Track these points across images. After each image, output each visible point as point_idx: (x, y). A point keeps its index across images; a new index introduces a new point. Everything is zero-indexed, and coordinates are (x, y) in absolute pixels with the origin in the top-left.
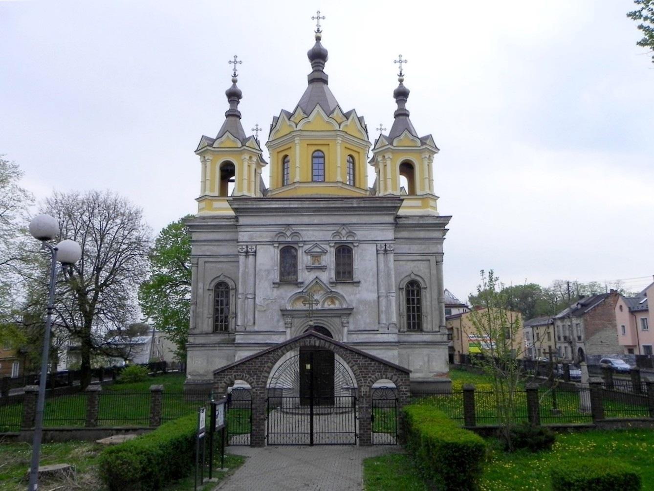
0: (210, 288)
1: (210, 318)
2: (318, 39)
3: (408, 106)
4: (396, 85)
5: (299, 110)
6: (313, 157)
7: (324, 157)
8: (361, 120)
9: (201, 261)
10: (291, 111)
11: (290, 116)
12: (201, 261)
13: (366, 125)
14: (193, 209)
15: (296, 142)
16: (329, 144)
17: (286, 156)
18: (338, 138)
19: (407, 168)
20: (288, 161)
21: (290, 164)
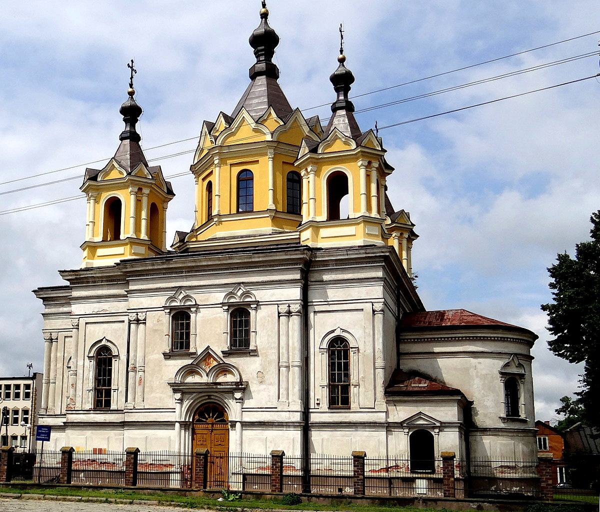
0: (91, 355)
9: (82, 321)
10: (215, 122)
14: (80, 261)
15: (216, 162)
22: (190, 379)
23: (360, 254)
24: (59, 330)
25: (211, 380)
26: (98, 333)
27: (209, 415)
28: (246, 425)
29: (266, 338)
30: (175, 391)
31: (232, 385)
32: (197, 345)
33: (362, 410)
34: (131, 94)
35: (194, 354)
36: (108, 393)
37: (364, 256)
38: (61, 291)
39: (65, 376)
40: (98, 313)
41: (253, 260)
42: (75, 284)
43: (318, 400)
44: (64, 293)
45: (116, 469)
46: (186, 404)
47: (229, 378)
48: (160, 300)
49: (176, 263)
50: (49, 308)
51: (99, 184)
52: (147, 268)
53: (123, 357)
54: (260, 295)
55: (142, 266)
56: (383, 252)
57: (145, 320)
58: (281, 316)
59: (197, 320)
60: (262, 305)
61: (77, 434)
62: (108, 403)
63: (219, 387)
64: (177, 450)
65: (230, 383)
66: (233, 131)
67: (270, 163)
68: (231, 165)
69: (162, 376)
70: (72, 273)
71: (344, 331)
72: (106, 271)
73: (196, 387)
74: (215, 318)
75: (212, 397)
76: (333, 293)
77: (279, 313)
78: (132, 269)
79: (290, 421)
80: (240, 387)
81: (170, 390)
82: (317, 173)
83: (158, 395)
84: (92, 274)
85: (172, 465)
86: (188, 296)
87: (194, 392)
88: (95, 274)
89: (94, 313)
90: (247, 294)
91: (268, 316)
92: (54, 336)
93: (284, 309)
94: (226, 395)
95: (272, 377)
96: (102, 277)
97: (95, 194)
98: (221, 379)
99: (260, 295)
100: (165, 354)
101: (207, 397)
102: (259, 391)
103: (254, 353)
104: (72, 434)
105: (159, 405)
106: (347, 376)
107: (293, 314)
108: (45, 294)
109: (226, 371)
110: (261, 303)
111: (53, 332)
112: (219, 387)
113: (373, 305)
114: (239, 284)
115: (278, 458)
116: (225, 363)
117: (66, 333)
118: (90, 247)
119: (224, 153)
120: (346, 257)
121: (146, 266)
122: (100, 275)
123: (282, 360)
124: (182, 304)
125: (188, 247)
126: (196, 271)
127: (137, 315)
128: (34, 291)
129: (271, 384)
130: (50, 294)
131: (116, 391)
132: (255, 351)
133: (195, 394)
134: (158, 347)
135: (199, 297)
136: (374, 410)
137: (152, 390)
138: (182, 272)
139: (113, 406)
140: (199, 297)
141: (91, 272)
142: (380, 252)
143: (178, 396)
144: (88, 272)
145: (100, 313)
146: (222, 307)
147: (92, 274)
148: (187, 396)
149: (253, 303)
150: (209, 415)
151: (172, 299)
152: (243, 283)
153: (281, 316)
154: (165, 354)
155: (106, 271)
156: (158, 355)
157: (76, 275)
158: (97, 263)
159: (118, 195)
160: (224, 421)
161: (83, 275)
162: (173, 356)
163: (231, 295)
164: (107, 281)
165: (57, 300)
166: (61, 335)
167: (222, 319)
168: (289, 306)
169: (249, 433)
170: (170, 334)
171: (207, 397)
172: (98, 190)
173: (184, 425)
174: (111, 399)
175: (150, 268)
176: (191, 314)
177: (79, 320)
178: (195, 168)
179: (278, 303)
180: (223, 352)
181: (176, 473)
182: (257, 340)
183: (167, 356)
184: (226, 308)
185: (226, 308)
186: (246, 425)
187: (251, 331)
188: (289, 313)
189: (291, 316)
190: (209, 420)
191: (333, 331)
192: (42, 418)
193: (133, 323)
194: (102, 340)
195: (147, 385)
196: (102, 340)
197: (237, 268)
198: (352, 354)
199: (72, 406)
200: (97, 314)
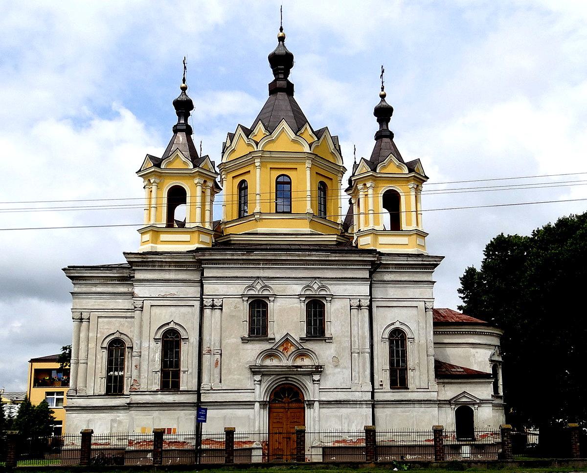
0: (157, 337)
1: (156, 372)
2: (281, 39)
3: (392, 126)
4: (377, 101)
5: (260, 125)
6: (277, 183)
7: (290, 183)
8: (335, 140)
11: (248, 132)
12: (147, 304)
13: (339, 146)
14: (139, 245)
15: (257, 164)
16: (297, 169)
17: (243, 181)
18: (307, 161)
19: (392, 201)
20: (246, 188)
21: (249, 190)
22: (268, 362)
23: (418, 261)
24: (92, 310)
25: (290, 363)
26: (165, 316)
27: (284, 395)
28: (324, 404)
30: (254, 373)
31: (312, 368)
32: (276, 331)
33: (419, 390)
34: (184, 89)
35: (274, 339)
37: (421, 263)
39: (98, 357)
40: (165, 296)
41: (330, 259)
42: (139, 267)
43: (381, 381)
44: (102, 273)
45: (186, 447)
46: (265, 385)
47: (307, 362)
48: (238, 288)
49: (256, 255)
50: (79, 287)
51: (163, 171)
53: (194, 339)
54: (335, 289)
55: (222, 255)
56: (435, 261)
58: (353, 309)
59: (274, 308)
60: (336, 298)
61: (143, 414)
63: (299, 370)
64: (257, 429)
65: (310, 367)
66: (273, 138)
67: (308, 172)
68: (270, 168)
69: (240, 359)
71: (402, 324)
73: (277, 370)
74: (293, 307)
75: (289, 379)
76: (393, 292)
77: (351, 306)
79: (362, 399)
80: (319, 370)
81: (248, 374)
82: (375, 188)
83: (235, 377)
84: (161, 258)
85: (251, 442)
86: (266, 286)
87: (273, 375)
88: (165, 258)
90: (322, 288)
91: (341, 309)
92: (85, 316)
93: (355, 303)
94: (304, 378)
95: (345, 361)
96: (170, 262)
97: (157, 181)
98: (299, 362)
99: (335, 289)
100: (243, 339)
101: (284, 379)
102: (334, 374)
104: (136, 415)
105: (237, 386)
106: (405, 361)
108: (77, 273)
109: (304, 355)
110: (334, 297)
111: (84, 312)
112: (299, 370)
113: (425, 304)
114: (315, 278)
115: (438, 432)
116: (303, 348)
117: (100, 313)
118: (154, 231)
119: (266, 158)
122: (169, 260)
123: (354, 347)
124: (261, 294)
125: (231, 239)
126: (274, 264)
127: (213, 300)
128: (64, 270)
129: (345, 368)
130: (84, 273)
131: (186, 372)
132: (331, 338)
133: (272, 377)
134: (236, 332)
135: (276, 287)
137: (230, 372)
138: (259, 264)
139: (181, 388)
140: (276, 287)
141: (161, 257)
142: (433, 261)
143: (258, 378)
144: (157, 256)
145: (167, 296)
146: (299, 298)
147: (161, 258)
148: (266, 378)
149: (328, 296)
151: (251, 287)
152: (319, 278)
153: (353, 309)
154: (243, 339)
156: (235, 340)
157: (143, 258)
158: (161, 248)
161: (150, 258)
163: (308, 287)
164: (175, 266)
165: (91, 280)
166: (94, 316)
167: (299, 309)
168: (360, 301)
169: (326, 411)
170: (248, 321)
171: (284, 379)
172: (160, 177)
173: (263, 404)
176: (268, 303)
177: (143, 303)
178: (225, 166)
179: (350, 297)
180: (301, 339)
181: (257, 448)
183: (244, 340)
184: (304, 299)
185: (304, 299)
186: (324, 404)
187: (326, 320)
188: (359, 307)
189: (361, 309)
191: (393, 324)
192: (71, 399)
193: (208, 308)
194: (170, 322)
196: (170, 322)
197: (313, 265)
198: (408, 344)
199: (136, 387)
200: (164, 298)
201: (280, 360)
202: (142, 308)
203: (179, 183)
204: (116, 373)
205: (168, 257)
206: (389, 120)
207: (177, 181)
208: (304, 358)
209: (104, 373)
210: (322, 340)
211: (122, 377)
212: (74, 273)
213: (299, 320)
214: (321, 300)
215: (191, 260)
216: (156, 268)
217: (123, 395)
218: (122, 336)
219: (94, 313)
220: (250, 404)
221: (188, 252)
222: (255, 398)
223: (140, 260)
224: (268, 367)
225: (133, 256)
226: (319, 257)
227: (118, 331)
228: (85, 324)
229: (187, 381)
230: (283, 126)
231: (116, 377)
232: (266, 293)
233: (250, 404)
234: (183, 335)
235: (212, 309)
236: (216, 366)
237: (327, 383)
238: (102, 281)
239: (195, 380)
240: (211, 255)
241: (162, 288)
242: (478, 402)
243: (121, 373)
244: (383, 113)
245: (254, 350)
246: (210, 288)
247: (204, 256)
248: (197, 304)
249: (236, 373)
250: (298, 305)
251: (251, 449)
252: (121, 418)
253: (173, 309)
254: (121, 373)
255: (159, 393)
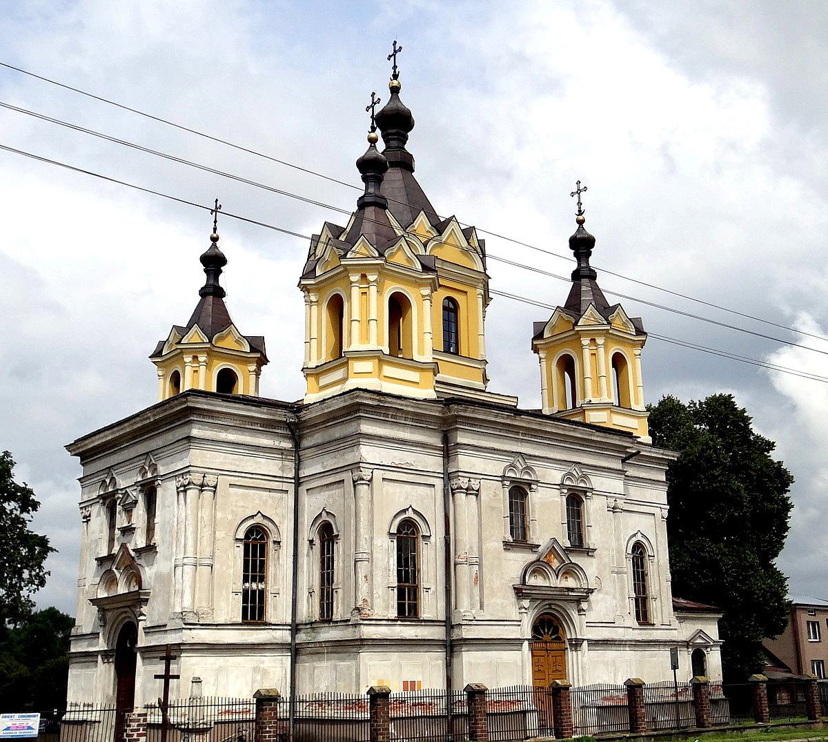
12: (378, 474)
23: (658, 453)
27: (549, 630)
29: (600, 536)
36: (414, 592)
38: (237, 405)
40: (399, 466)
47: (571, 583)
50: (199, 429)
52: (489, 418)
54: (599, 482)
55: (484, 414)
57: (478, 491)
59: (536, 498)
62: (414, 609)
63: (570, 594)
69: (503, 573)
70: (375, 397)
71: (643, 536)
72: (423, 406)
73: (549, 593)
74: (553, 501)
78: (471, 415)
79: (624, 639)
81: (512, 593)
83: (499, 601)
84: (402, 405)
86: (528, 467)
87: (538, 599)
88: (406, 406)
89: (393, 465)
90: (584, 477)
96: (408, 412)
103: (589, 552)
104: (370, 659)
107: (618, 510)
112: (570, 594)
117: (232, 478)
120: (648, 454)
121: (488, 415)
126: (532, 436)
133: (539, 601)
136: (671, 628)
138: (518, 433)
139: (425, 614)
143: (526, 603)
144: (399, 401)
145: (402, 466)
147: (402, 405)
150: (549, 630)
154: (506, 544)
155: (423, 406)
157: (379, 401)
159: (408, 294)
160: (559, 639)
161: (389, 403)
162: (515, 546)
164: (412, 420)
166: (223, 481)
167: (558, 501)
171: (548, 607)
174: (398, 600)
175: (493, 419)
177: (372, 473)
179: (606, 495)
182: (593, 538)
190: (546, 637)
192: (190, 629)
194: (408, 509)
195: (486, 585)
196: (408, 509)
197: (571, 443)
199: (368, 612)
201: (546, 576)
202: (371, 480)
203: (402, 289)
204: (254, 586)
205: (412, 404)
206: (589, 254)
207: (403, 287)
208: (568, 576)
209: (239, 586)
210: (583, 552)
211: (262, 592)
212: (202, 403)
213: (560, 521)
214: (580, 494)
215: (437, 414)
216: (390, 420)
217: (266, 624)
218: (265, 522)
219: (224, 477)
220: (514, 643)
221: (425, 400)
222: (522, 633)
223: (376, 403)
224: (541, 588)
225: (368, 395)
226: (582, 434)
227: (259, 512)
228: (208, 495)
229: (431, 605)
230: (453, 227)
231: (254, 592)
232: (526, 477)
233: (514, 643)
234: (423, 530)
235: (467, 494)
236: (476, 584)
237: (591, 616)
238: (237, 423)
239: (442, 604)
240: (473, 412)
241: (396, 453)
242: (712, 644)
243: (261, 586)
244: (582, 245)
245: (519, 560)
246: (465, 461)
247: (465, 411)
248: (439, 483)
249: (499, 594)
250: (558, 499)
251: (524, 712)
252: (269, 665)
253: (408, 487)
254: (261, 586)
255: (399, 623)
